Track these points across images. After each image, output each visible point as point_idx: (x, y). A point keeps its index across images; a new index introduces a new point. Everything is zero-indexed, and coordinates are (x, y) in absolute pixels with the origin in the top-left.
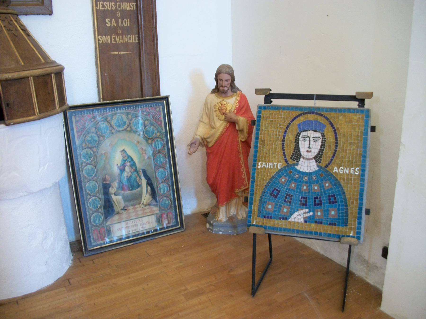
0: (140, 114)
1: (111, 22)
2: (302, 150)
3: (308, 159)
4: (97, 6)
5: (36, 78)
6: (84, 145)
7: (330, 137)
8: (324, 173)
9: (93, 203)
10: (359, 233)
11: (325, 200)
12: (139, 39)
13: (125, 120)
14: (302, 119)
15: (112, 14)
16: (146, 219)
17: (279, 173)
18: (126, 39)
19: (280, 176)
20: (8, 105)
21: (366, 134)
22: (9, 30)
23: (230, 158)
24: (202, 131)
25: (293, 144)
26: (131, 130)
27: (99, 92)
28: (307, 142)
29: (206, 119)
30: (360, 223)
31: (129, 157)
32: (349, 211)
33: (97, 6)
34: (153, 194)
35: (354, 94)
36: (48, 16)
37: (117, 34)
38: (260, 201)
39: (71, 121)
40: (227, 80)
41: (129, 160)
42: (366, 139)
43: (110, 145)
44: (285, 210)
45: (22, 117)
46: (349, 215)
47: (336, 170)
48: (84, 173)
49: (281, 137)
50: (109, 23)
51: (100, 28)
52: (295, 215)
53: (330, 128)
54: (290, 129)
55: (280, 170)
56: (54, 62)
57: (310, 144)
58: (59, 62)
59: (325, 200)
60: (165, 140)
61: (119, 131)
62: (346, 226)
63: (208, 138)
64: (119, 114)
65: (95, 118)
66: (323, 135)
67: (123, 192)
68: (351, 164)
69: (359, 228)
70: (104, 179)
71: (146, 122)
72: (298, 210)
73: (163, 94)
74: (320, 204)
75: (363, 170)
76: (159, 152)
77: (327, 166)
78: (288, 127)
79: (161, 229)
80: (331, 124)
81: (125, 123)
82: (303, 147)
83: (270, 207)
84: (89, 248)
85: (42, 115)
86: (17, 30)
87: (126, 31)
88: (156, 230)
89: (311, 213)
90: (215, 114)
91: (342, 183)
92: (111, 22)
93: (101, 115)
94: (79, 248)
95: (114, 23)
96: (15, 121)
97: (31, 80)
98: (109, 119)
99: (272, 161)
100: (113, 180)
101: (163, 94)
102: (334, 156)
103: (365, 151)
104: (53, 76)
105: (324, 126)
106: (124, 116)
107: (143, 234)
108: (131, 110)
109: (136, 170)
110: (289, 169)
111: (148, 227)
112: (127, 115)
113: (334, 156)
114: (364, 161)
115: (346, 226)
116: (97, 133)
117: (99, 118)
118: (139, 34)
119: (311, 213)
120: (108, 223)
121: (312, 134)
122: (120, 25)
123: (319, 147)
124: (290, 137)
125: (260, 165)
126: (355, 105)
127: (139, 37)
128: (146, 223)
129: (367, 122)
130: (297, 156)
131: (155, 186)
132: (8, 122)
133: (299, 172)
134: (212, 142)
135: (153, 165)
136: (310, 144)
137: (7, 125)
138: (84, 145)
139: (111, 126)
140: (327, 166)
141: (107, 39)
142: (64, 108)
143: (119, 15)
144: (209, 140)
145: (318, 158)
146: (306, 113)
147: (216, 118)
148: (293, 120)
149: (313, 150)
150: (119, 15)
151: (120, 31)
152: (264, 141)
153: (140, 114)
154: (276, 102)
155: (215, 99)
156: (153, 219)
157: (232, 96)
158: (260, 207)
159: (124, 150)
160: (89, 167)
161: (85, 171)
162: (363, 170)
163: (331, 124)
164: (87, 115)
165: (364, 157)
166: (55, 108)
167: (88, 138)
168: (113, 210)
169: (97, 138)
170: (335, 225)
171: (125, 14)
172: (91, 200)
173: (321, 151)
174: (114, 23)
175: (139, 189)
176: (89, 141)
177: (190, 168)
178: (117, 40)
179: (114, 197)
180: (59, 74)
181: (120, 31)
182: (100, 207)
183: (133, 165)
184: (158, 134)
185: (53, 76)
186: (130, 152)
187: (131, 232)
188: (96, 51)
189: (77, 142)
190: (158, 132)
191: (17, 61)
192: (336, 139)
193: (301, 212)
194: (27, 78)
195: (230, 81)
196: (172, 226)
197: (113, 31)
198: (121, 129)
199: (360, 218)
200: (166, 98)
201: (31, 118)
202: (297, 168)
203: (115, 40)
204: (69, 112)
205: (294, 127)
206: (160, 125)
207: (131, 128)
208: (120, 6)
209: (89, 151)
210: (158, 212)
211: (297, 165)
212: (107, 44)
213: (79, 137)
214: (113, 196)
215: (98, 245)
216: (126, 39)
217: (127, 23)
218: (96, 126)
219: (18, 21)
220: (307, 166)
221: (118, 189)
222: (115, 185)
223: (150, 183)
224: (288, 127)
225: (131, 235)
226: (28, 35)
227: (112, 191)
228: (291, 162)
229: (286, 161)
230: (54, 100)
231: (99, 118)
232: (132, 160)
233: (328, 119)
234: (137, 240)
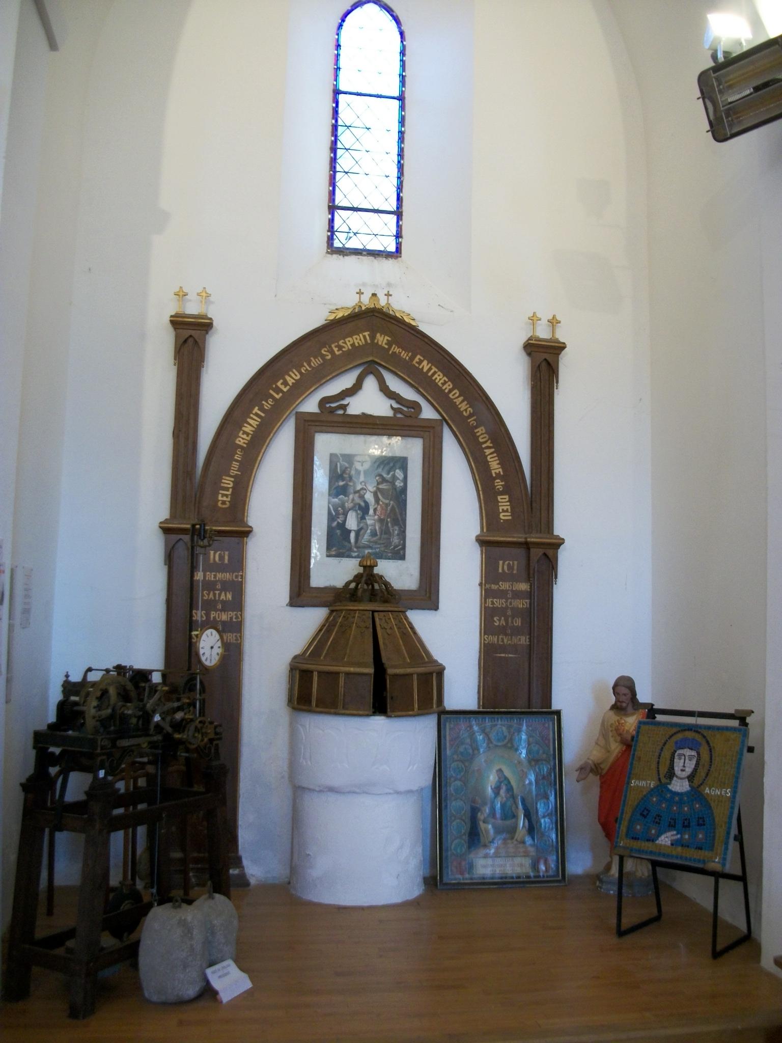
0: (524, 728)
1: (500, 620)
2: (676, 768)
3: (681, 779)
4: (485, 603)
5: (419, 675)
6: (455, 757)
7: (705, 756)
8: (696, 793)
9: (456, 828)
10: (724, 859)
11: (694, 823)
12: (530, 641)
13: (506, 733)
14: (680, 736)
15: (501, 612)
16: (518, 860)
17: (651, 792)
18: (515, 640)
19: (652, 796)
20: (392, 698)
21: (742, 754)
22: (399, 628)
23: (611, 778)
24: (596, 755)
25: (668, 762)
26: (512, 746)
27: (479, 698)
28: (682, 761)
29: (602, 742)
30: (726, 849)
31: (506, 778)
32: (717, 835)
33: (485, 603)
34: (532, 829)
35: (732, 712)
36: (433, 612)
37: (506, 635)
38: (630, 821)
39: (445, 728)
40: (625, 695)
41: (506, 782)
42: (740, 759)
43: (486, 761)
44: (653, 832)
45: (402, 711)
46: (716, 841)
47: (707, 791)
48: (451, 789)
49: (657, 754)
50: (497, 622)
51: (487, 627)
52: (663, 837)
53: (706, 747)
54: (667, 746)
55: (652, 790)
56: (436, 661)
57: (685, 763)
58: (440, 661)
59: (694, 823)
60: (552, 764)
61: (497, 746)
62: (712, 850)
63: (601, 763)
64: (501, 726)
65: (471, 727)
66: (698, 754)
67: (493, 821)
68: (722, 785)
69: (725, 854)
70: (474, 801)
71: (531, 739)
72: (665, 832)
73: (555, 706)
74: (688, 826)
75: (734, 792)
76: (544, 778)
77: (699, 786)
78: (665, 743)
79: (535, 877)
80: (708, 742)
81: (505, 737)
82: (678, 765)
83: (638, 827)
84: (445, 880)
85: (420, 712)
86: (406, 628)
87: (516, 631)
88: (529, 877)
89: (679, 836)
90: (611, 734)
91: (712, 804)
92: (500, 620)
93: (478, 725)
94: (434, 881)
95: (503, 622)
96: (396, 714)
97: (415, 677)
98: (488, 730)
99: (645, 780)
100: (485, 804)
101: (555, 706)
102: (707, 775)
103: (738, 772)
104: (434, 675)
105: (700, 744)
106: (504, 729)
107: (512, 878)
108: (515, 722)
109: (513, 797)
110: (662, 788)
111: (518, 870)
112: (509, 727)
113: (707, 775)
114: (737, 782)
115: (712, 850)
116: (471, 745)
117: (476, 728)
118: (530, 634)
119: (679, 836)
120: (472, 856)
121: (687, 752)
122: (510, 624)
123: (693, 766)
124: (666, 754)
125: (633, 783)
126: (735, 723)
127: (530, 639)
128: (516, 866)
129: (743, 742)
130: (671, 774)
131: (534, 818)
132: (389, 713)
133: (671, 792)
134: (605, 767)
135: (534, 793)
136: (685, 763)
137: (389, 717)
138: (455, 757)
139: (489, 739)
140: (699, 786)
141: (494, 639)
142: (440, 709)
143: (509, 613)
144: (602, 766)
145: (691, 778)
146: (685, 730)
147: (611, 740)
148: (671, 737)
149: (687, 769)
150: (509, 613)
151: (509, 631)
152: (640, 758)
153: (524, 728)
154: (659, 718)
155: (613, 717)
156: (527, 862)
157: (632, 714)
158: (628, 828)
159: (500, 771)
160: (458, 783)
161: (453, 787)
162: (734, 792)
163: (708, 742)
164: (462, 724)
165: (737, 778)
166: (432, 707)
167: (461, 749)
168: (479, 840)
169: (470, 751)
170: (701, 849)
171: (516, 612)
172: (454, 823)
173: (695, 770)
174: (503, 622)
175: (514, 820)
176: (462, 753)
177: (581, 800)
178: (505, 641)
179: (482, 825)
180: (440, 672)
181: (509, 631)
182: (465, 834)
183: (510, 789)
184: (544, 756)
185: (434, 675)
186: (508, 773)
187: (498, 872)
188: (480, 652)
189: (448, 752)
190: (544, 753)
191: (404, 658)
192: (711, 759)
193: (669, 834)
194: (411, 675)
195: (629, 696)
196: (550, 876)
197: (502, 630)
198: (499, 744)
199: (727, 844)
200: (558, 713)
201: (411, 713)
202: (670, 787)
203: (503, 641)
204: (444, 716)
205: (671, 744)
206: (548, 746)
207: (512, 744)
208: (511, 603)
209: (460, 764)
210: (534, 854)
211: (670, 784)
212: (493, 645)
213: (451, 745)
214: (481, 823)
215: (455, 879)
216: (515, 640)
217: (518, 622)
218: (472, 736)
219: (406, 618)
220: (679, 786)
221: (489, 815)
222: (487, 810)
223: (528, 815)
224: (665, 743)
225: (497, 876)
226: (415, 633)
227: (481, 816)
228: (664, 780)
229: (660, 780)
230: (432, 699)
231: (476, 728)
232: (509, 782)
233: (704, 737)
234: (504, 884)
